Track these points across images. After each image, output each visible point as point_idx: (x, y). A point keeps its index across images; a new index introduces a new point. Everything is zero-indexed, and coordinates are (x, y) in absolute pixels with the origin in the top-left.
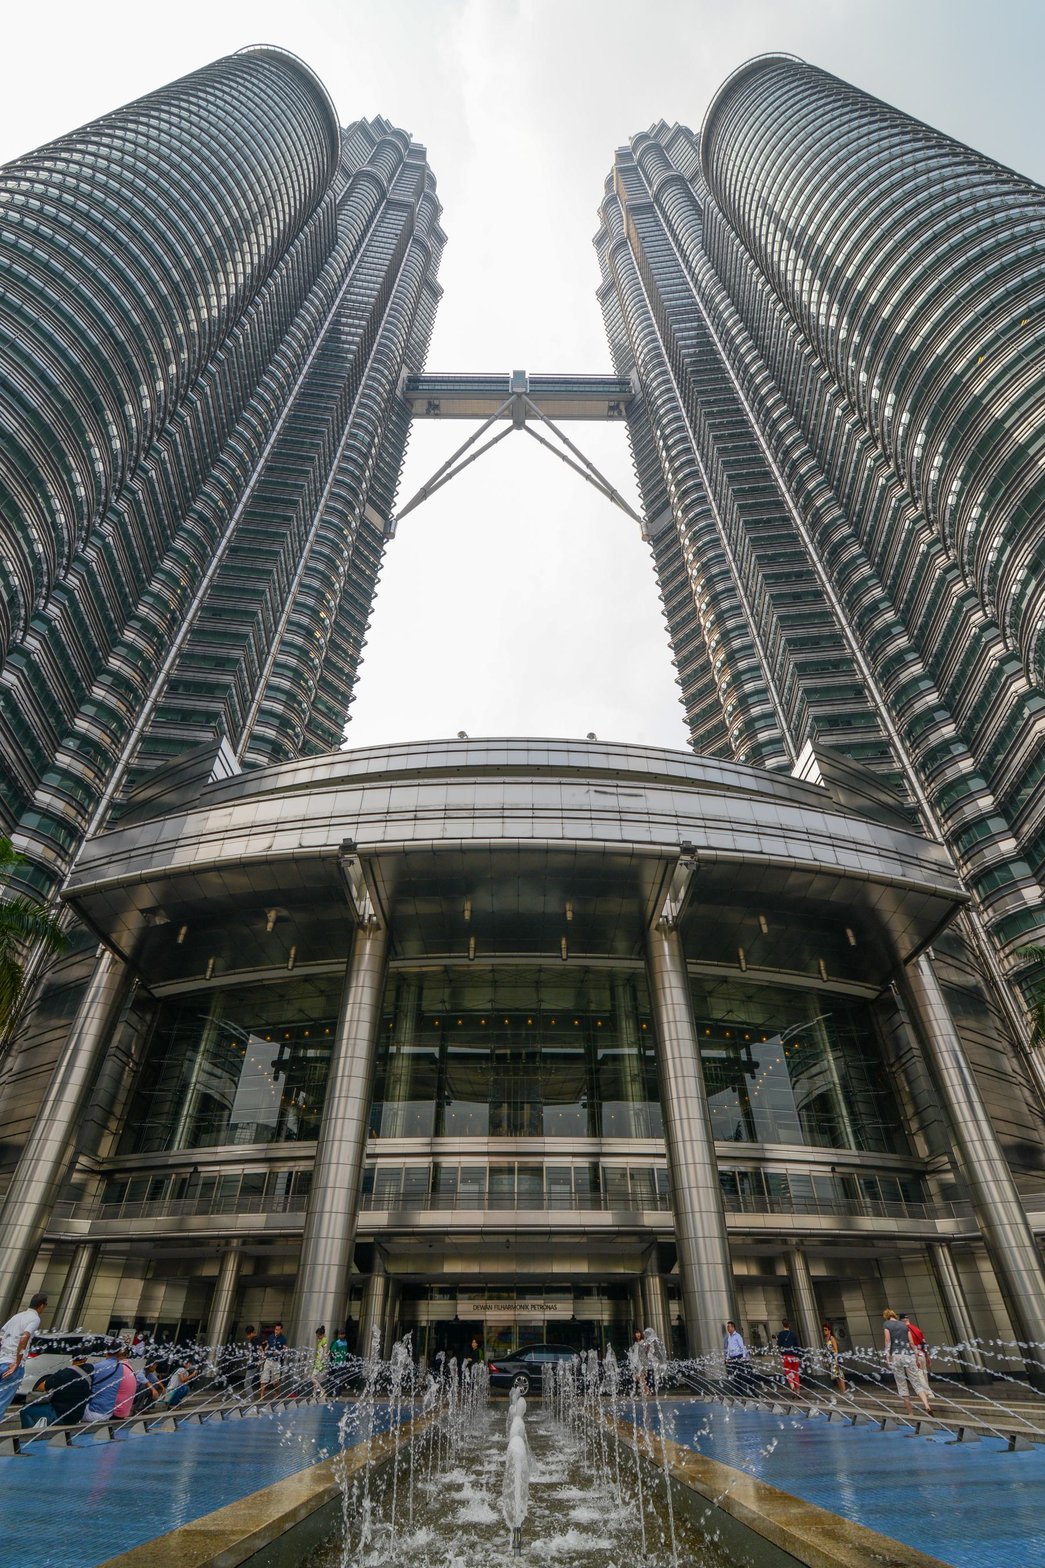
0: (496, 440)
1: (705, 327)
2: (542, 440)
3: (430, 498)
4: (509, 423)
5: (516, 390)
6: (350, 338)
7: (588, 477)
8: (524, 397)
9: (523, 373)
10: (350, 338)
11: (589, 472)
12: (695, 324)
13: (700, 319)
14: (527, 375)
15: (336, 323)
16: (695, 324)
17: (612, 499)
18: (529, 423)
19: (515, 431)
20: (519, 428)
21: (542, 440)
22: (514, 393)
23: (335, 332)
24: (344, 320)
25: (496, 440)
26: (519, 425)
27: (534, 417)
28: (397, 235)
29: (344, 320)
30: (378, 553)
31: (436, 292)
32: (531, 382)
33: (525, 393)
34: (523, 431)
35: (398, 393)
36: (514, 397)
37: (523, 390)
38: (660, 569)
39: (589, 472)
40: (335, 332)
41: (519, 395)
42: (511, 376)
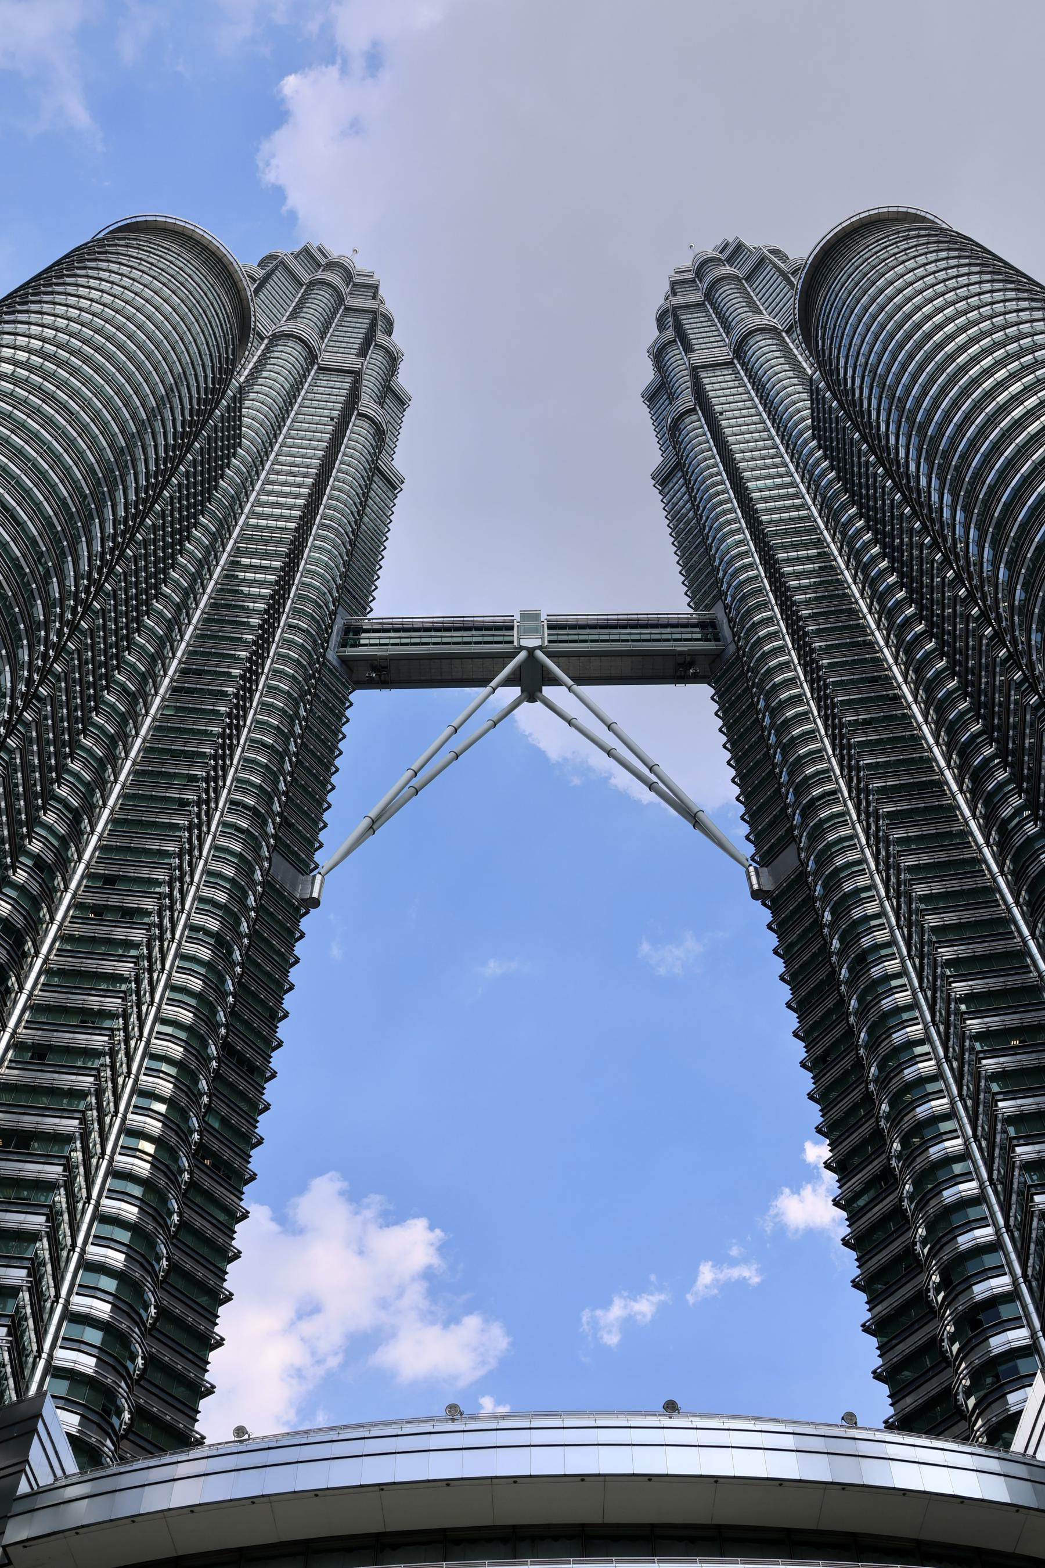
1: (832, 569)
4: (515, 692)
5: (524, 643)
6: (255, 590)
9: (536, 616)
10: (255, 590)
11: (654, 778)
12: (813, 552)
13: (820, 543)
15: (229, 576)
16: (813, 552)
18: (548, 691)
19: (526, 705)
20: (532, 699)
22: (522, 648)
23: (230, 585)
24: (245, 561)
26: (531, 695)
27: (555, 682)
28: (332, 419)
29: (245, 561)
30: (292, 935)
31: (393, 485)
32: (550, 627)
33: (540, 648)
34: (538, 704)
35: (331, 655)
36: (523, 655)
37: (537, 643)
38: (788, 949)
39: (654, 778)
40: (230, 585)
41: (531, 651)
42: (517, 618)
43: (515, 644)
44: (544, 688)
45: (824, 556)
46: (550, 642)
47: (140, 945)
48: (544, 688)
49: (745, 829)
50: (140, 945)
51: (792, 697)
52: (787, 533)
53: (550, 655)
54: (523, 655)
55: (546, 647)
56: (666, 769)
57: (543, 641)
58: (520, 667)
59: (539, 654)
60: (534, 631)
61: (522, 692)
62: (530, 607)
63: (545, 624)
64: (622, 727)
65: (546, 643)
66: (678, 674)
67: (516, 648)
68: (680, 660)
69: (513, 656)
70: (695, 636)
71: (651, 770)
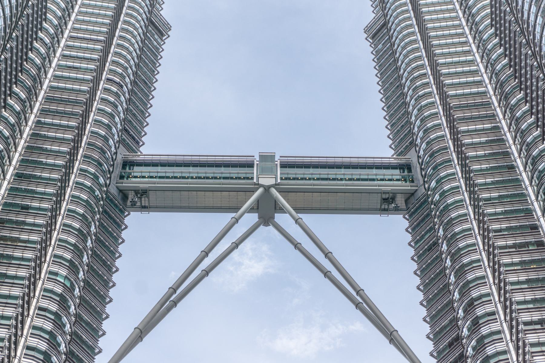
0: (236, 245)
2: (297, 246)
3: (147, 339)
5: (262, 181)
7: (357, 305)
8: (273, 191)
14: (277, 158)
17: (391, 341)
18: (279, 218)
21: (297, 246)
25: (236, 245)
34: (271, 228)
36: (261, 190)
37: (272, 181)
41: (267, 189)
43: (255, 180)
44: (276, 215)
45: (497, 129)
46: (281, 179)
47: (4, 339)
48: (276, 215)
49: (430, 346)
50: (4, 339)
51: (435, 126)
52: (468, 107)
53: (280, 191)
54: (261, 190)
55: (278, 184)
56: (370, 293)
57: (276, 180)
58: (258, 201)
59: (273, 191)
60: (271, 171)
61: (259, 218)
62: (267, 150)
63: (278, 163)
64: (337, 255)
65: (279, 181)
66: (383, 207)
67: (255, 184)
68: (384, 196)
69: (253, 191)
70: (395, 177)
71: (358, 293)
